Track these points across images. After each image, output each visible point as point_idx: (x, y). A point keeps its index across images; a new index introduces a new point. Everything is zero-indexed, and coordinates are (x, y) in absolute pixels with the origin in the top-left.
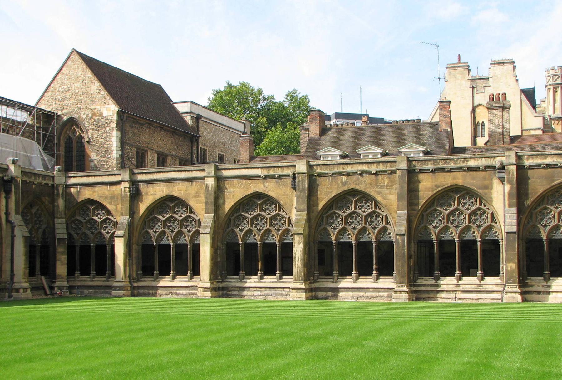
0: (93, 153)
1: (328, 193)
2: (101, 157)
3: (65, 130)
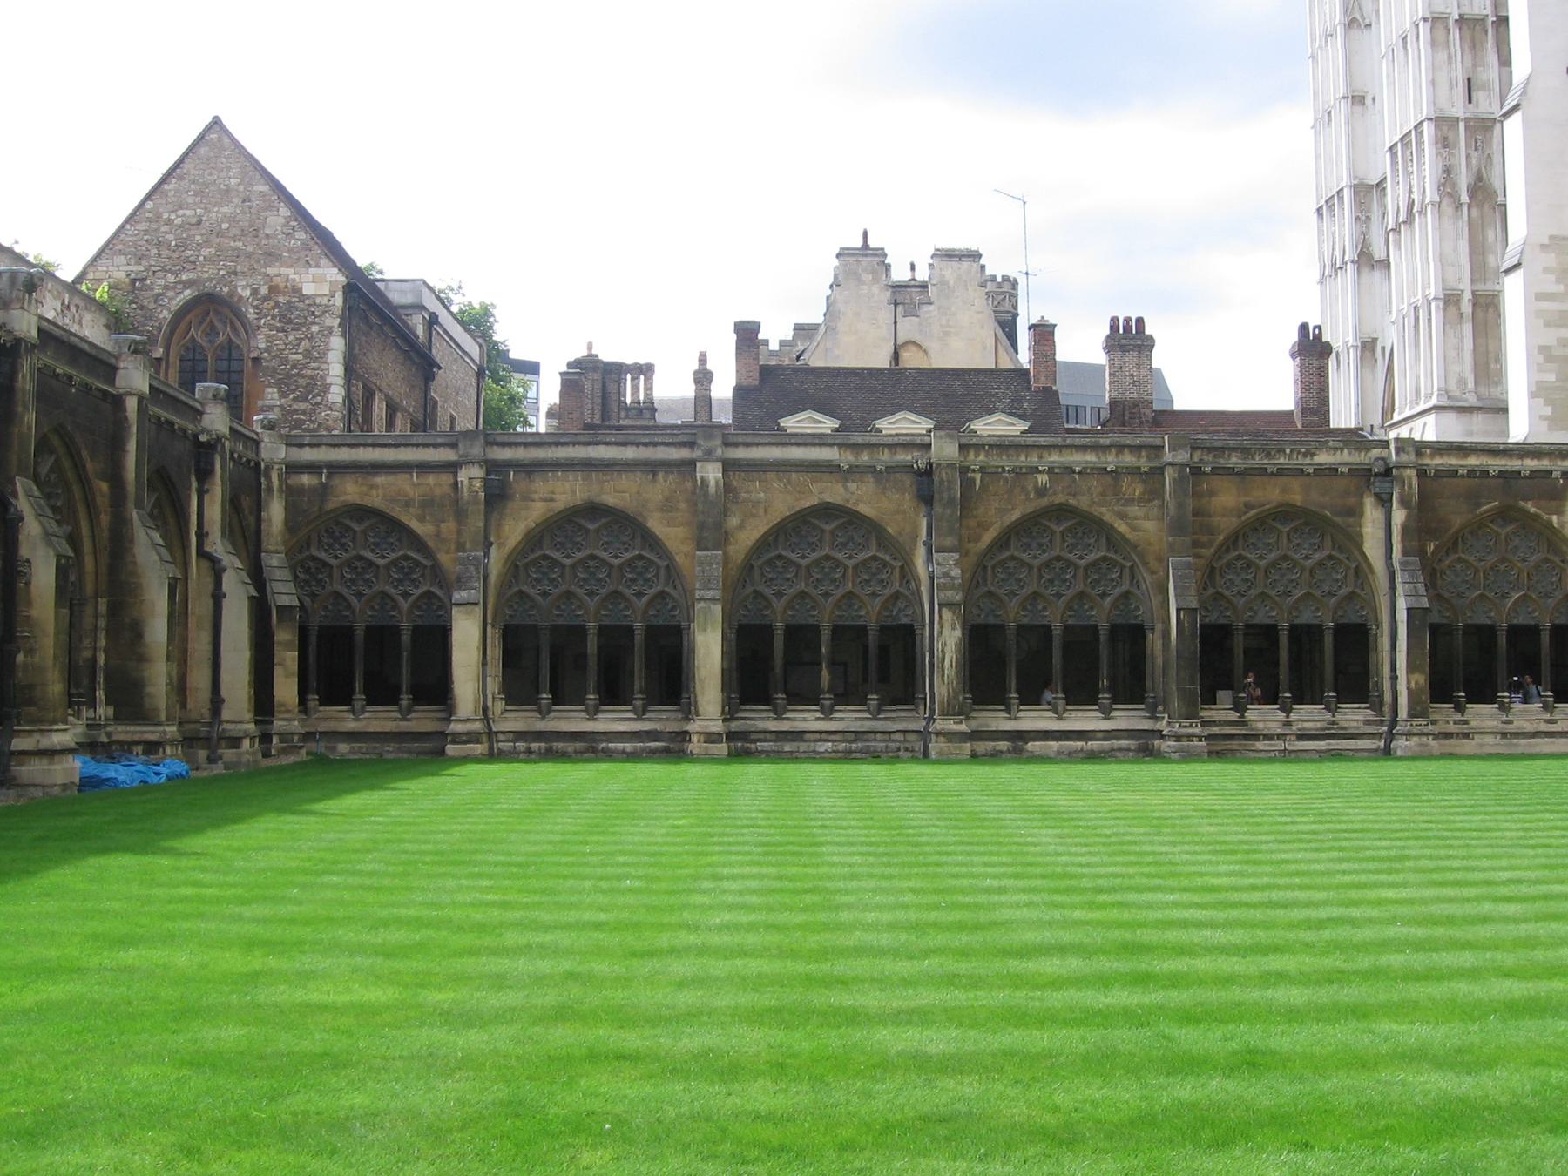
0: (270, 390)
2: (295, 399)
3: (183, 326)
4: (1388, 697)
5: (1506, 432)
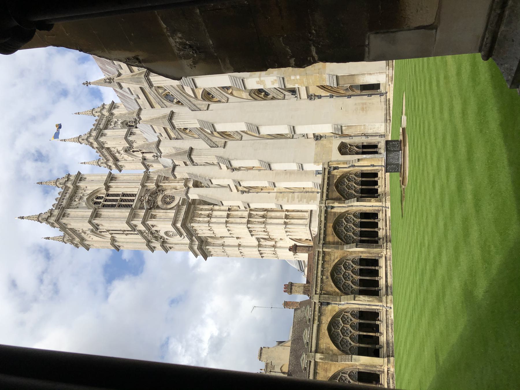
1: (332, 287)
4: (377, 208)
5: (316, 211)
